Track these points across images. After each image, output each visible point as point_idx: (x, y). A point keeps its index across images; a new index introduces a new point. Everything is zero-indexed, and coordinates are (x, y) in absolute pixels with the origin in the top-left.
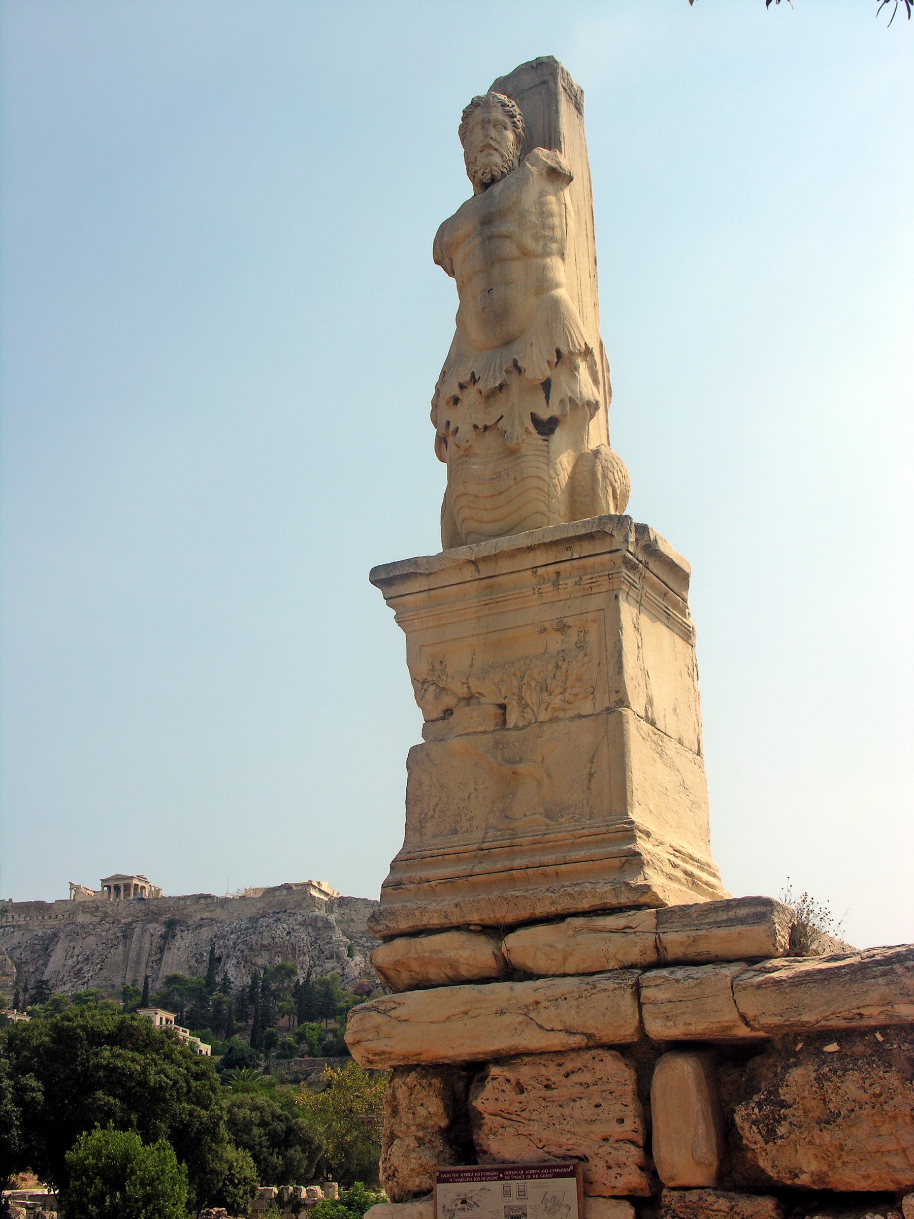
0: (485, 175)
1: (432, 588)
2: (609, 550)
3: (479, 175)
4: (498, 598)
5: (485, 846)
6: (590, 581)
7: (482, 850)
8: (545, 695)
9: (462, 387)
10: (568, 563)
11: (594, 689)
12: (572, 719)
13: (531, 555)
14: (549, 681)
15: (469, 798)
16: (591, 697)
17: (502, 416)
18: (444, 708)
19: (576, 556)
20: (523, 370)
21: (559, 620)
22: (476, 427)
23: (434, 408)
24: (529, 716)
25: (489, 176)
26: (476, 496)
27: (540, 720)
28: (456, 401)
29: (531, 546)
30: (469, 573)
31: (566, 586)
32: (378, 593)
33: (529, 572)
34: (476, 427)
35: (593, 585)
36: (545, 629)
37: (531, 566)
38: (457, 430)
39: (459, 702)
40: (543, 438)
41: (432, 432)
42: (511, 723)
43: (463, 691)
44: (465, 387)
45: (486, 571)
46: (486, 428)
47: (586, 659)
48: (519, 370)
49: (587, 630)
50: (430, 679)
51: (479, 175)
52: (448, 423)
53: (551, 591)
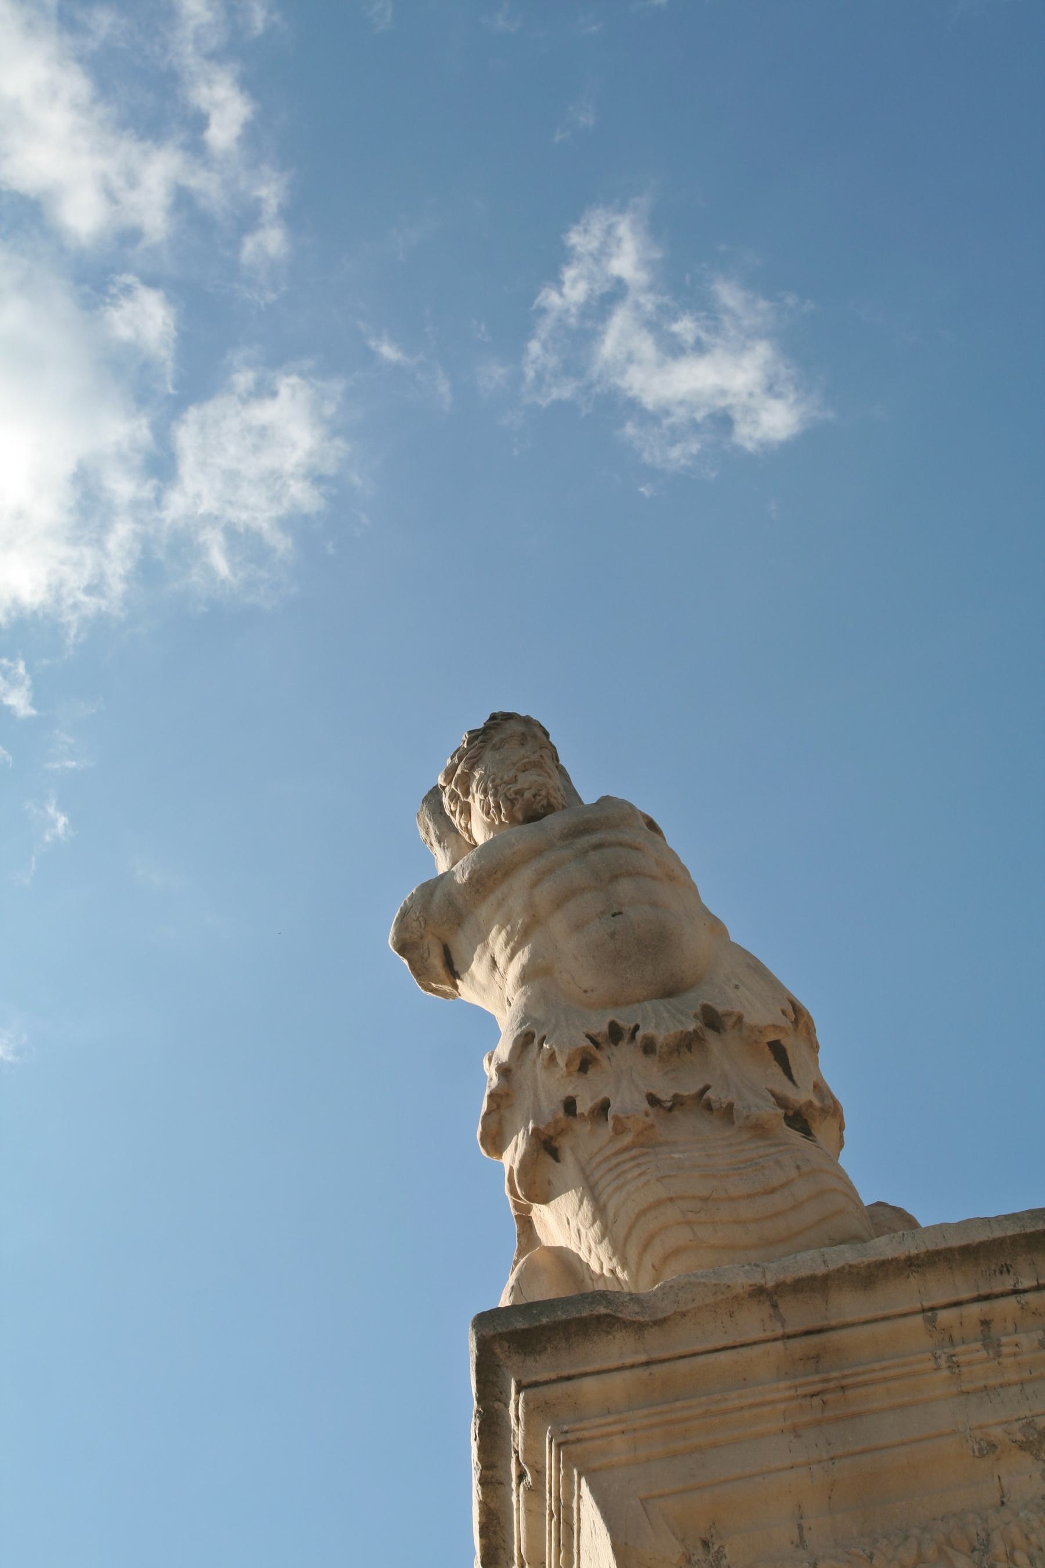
0: (538, 798)
1: (655, 1356)
4: (844, 1377)
17: (707, 1088)
19: (1026, 1283)
21: (1024, 1421)
22: (653, 1100)
23: (495, 1106)
25: (545, 802)
26: (705, 1200)
31: (1016, 1349)
34: (653, 1100)
36: (992, 1446)
38: (604, 1107)
46: (678, 1102)
51: (528, 795)
52: (570, 1106)
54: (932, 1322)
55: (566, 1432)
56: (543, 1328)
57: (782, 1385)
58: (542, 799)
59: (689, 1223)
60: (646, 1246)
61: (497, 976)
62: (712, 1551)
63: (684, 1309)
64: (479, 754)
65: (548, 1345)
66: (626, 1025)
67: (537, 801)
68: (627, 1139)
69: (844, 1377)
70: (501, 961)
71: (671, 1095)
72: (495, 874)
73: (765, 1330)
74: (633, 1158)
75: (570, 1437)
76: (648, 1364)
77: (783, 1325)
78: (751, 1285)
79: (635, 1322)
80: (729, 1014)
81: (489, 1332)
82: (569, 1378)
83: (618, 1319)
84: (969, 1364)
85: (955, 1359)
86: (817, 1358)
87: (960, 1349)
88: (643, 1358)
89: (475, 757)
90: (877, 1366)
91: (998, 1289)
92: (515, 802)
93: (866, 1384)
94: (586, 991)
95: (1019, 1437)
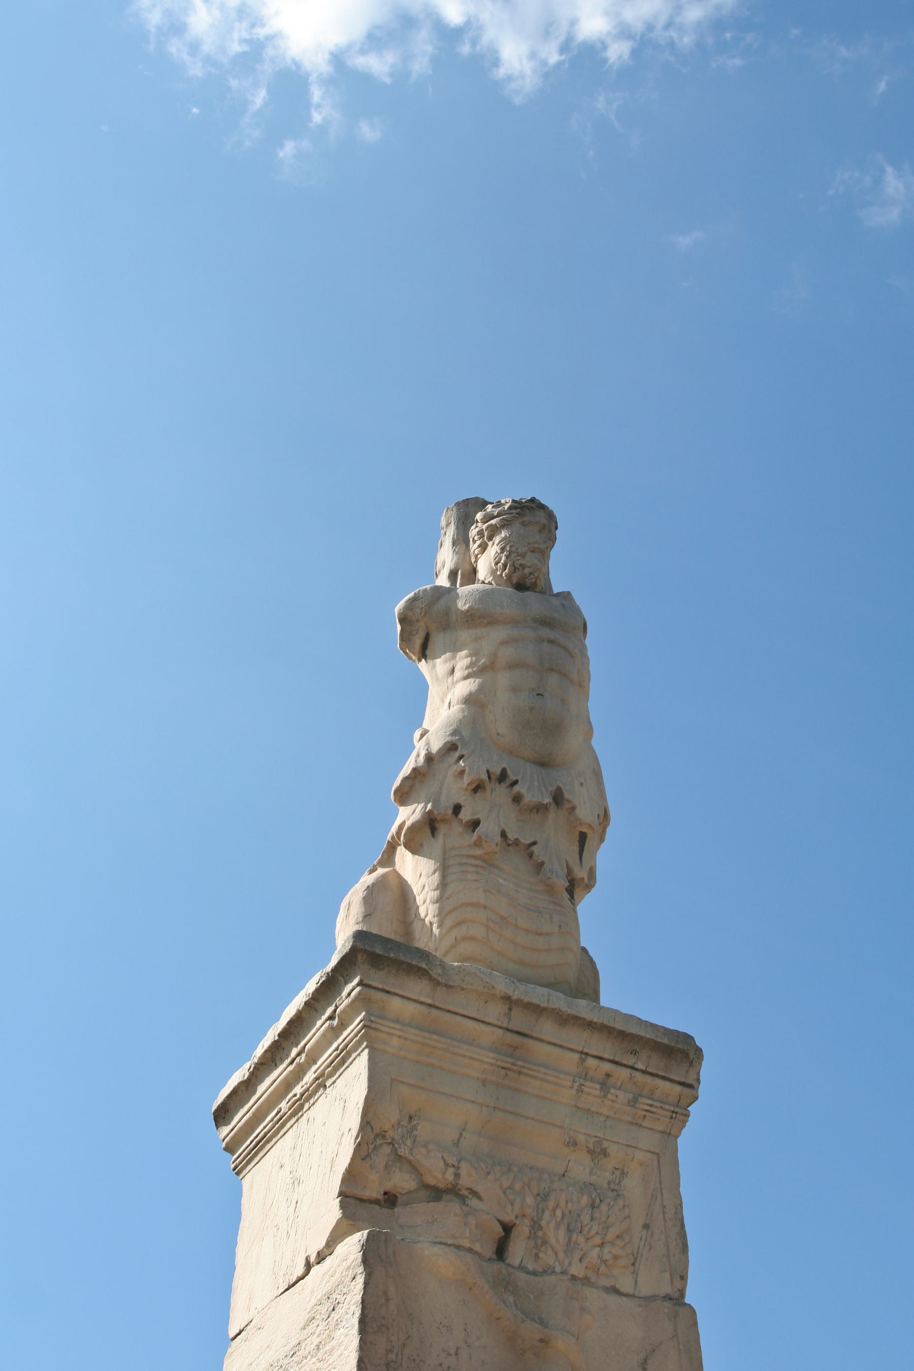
0: (532, 576)
1: (437, 1004)
2: (683, 1080)
3: (527, 571)
4: (524, 1067)
6: (647, 1108)
13: (586, 1034)
15: (456, 1354)
16: (632, 1269)
17: (534, 843)
18: (388, 1186)
19: (640, 1066)
21: (598, 1139)
22: (504, 834)
24: (548, 1258)
25: (533, 581)
26: (503, 918)
29: (596, 1023)
30: (494, 1012)
35: (648, 1114)
36: (575, 1144)
37: (580, 1049)
38: (475, 824)
46: (517, 842)
49: (626, 1170)
50: (391, 1133)
51: (527, 571)
52: (457, 809)
53: (595, 1096)
54: (583, 1061)
55: (372, 1021)
56: (389, 958)
57: (491, 1055)
59: (488, 927)
60: (458, 924)
61: (450, 680)
62: (412, 1124)
63: (465, 987)
64: (511, 521)
65: (386, 968)
66: (512, 777)
67: (530, 578)
68: (478, 852)
69: (524, 1067)
70: (458, 674)
71: (515, 838)
72: (484, 619)
73: (498, 1020)
74: (476, 866)
75: (373, 1025)
76: (430, 1006)
77: (508, 1022)
78: (505, 993)
79: (436, 979)
80: (569, 801)
81: (360, 946)
82: (388, 992)
83: (428, 974)
84: (588, 1094)
85: (583, 1087)
86: (516, 1048)
87: (588, 1084)
88: (430, 1001)
89: (508, 521)
90: (543, 1070)
91: (625, 1062)
92: (517, 571)
93: (532, 1077)
94: (498, 734)
95: (591, 1146)
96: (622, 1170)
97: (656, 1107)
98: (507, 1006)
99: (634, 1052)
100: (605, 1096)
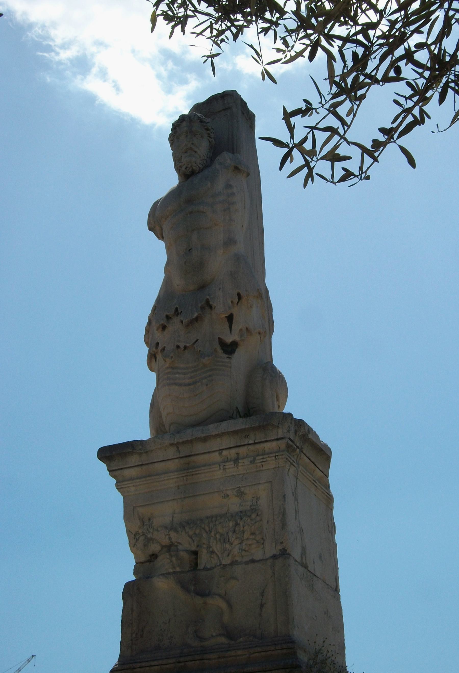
0: (187, 169)
1: (144, 463)
2: (276, 437)
5: (182, 659)
6: (261, 460)
7: (179, 662)
8: (228, 546)
9: (168, 318)
10: (245, 448)
11: (264, 541)
12: (247, 563)
14: (230, 534)
15: (169, 622)
16: (262, 546)
17: (197, 340)
18: (151, 553)
19: (251, 442)
20: (213, 307)
21: (238, 489)
22: (178, 347)
23: (147, 332)
25: (190, 170)
27: (223, 563)
28: (164, 328)
29: (218, 434)
30: (171, 453)
32: (103, 466)
33: (217, 454)
35: (263, 463)
36: (228, 496)
37: (218, 449)
39: (162, 549)
40: (227, 356)
41: (146, 350)
42: (201, 567)
43: (166, 541)
44: (171, 318)
45: (185, 450)
47: (258, 518)
48: (211, 307)
51: (183, 168)
52: (158, 344)
53: (233, 468)
58: (189, 169)
63: (152, 449)
69: (193, 472)
76: (142, 465)
77: (179, 454)
82: (122, 469)
84: (229, 468)
85: (224, 467)
93: (198, 474)
96: (257, 497)
97: (266, 458)
98: (176, 447)
99: (246, 436)
100: (238, 465)
